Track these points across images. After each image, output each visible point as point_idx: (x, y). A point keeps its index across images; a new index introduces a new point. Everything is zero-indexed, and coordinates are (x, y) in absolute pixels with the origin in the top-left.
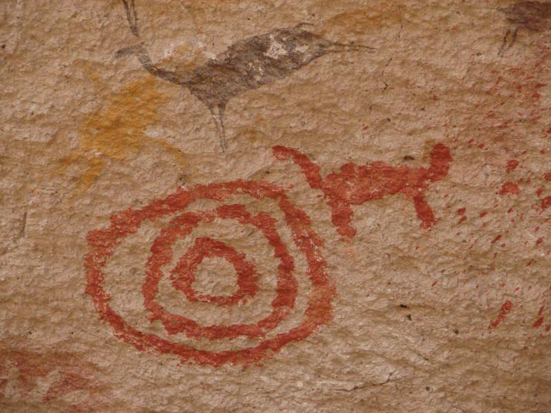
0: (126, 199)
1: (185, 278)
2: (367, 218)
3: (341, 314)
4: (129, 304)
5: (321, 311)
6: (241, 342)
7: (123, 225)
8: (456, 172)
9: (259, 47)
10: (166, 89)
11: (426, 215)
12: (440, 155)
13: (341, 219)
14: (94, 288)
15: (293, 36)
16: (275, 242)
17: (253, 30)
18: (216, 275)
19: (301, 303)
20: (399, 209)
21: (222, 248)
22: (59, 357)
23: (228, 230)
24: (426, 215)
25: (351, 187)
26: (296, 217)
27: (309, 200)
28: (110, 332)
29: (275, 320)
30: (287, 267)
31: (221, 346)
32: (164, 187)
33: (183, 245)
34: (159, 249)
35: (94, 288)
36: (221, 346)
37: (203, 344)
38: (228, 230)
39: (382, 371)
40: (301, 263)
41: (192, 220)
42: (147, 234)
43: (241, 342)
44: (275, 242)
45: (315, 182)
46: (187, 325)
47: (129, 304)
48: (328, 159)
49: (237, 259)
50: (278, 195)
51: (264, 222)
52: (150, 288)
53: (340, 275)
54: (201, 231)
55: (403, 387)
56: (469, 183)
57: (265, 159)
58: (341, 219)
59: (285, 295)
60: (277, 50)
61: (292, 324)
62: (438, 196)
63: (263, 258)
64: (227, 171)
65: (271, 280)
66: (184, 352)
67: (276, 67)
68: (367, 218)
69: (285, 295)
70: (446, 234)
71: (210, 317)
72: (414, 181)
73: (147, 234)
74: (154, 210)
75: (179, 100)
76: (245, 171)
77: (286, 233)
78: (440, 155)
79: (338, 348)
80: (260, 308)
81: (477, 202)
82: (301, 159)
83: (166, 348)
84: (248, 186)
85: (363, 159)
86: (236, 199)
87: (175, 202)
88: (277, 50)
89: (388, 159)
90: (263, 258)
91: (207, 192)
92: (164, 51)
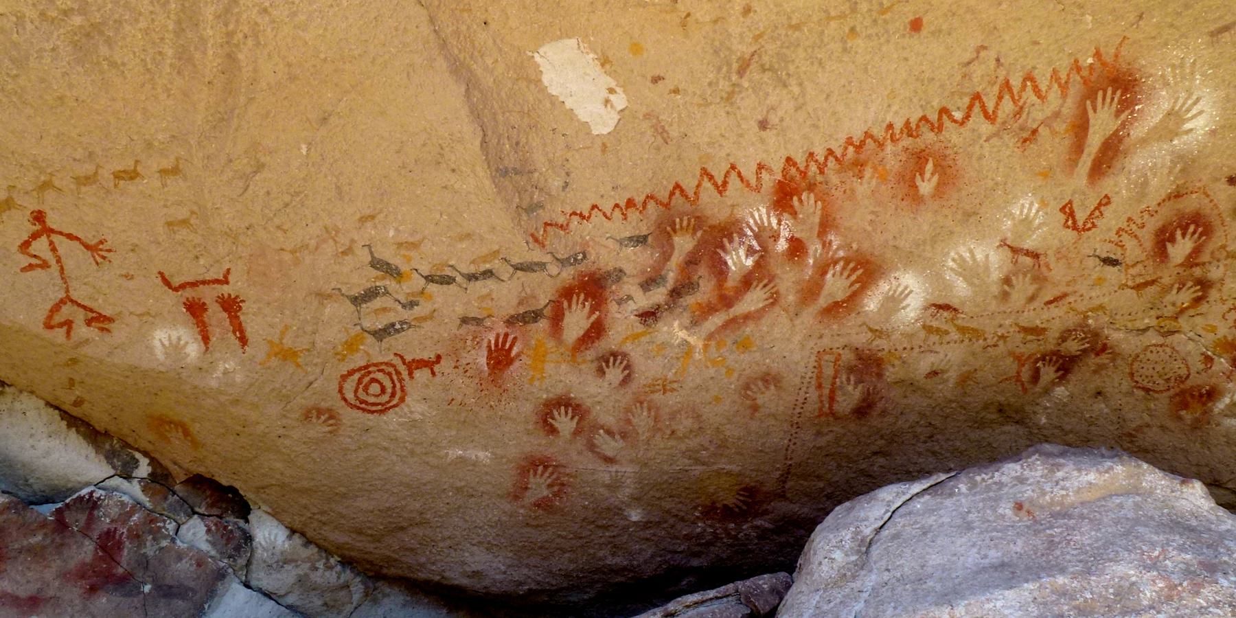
0: (352, 366)
1: (366, 389)
2: (417, 374)
3: (408, 399)
4: (350, 396)
5: (402, 400)
6: (379, 407)
7: (351, 373)
8: (443, 362)
9: (393, 325)
10: (366, 335)
11: (433, 373)
12: (439, 358)
13: (411, 374)
14: (340, 391)
15: (402, 323)
16: (392, 380)
17: (393, 320)
18: (375, 388)
19: (397, 397)
20: (427, 371)
21: (377, 381)
22: (329, 410)
23: (379, 376)
24: (433, 373)
25: (415, 365)
26: (398, 373)
27: (402, 369)
28: (343, 403)
29: (388, 402)
30: (394, 386)
31: (374, 408)
32: (363, 363)
33: (367, 379)
34: (360, 381)
35: (340, 391)
36: (374, 408)
37: (369, 408)
38: (379, 376)
39: (418, 417)
40: (398, 385)
41: (370, 373)
42: (357, 376)
43: (379, 407)
44: (392, 380)
45: (404, 363)
46: (366, 403)
47: (350, 396)
48: (408, 358)
49: (381, 384)
50: (394, 366)
51: (389, 374)
52: (356, 391)
53: (408, 388)
54: (372, 376)
55: (423, 421)
56: (445, 366)
57: (392, 357)
58: (411, 374)
59: (393, 395)
60: (398, 326)
61: (394, 402)
62: (436, 368)
63: (388, 384)
64: (381, 359)
65: (389, 390)
66: (364, 410)
67: (397, 331)
68: (417, 374)
69: (393, 395)
70: (438, 379)
71: (372, 400)
72: (429, 364)
73: (357, 376)
74: (360, 369)
75: (370, 339)
76: (386, 360)
77: (395, 377)
78: (439, 358)
79: (406, 410)
80: (385, 398)
81: (447, 371)
82: (401, 357)
83: (359, 408)
84: (386, 364)
85: (418, 358)
86: (383, 367)
87: (366, 367)
88: (398, 326)
89: (426, 358)
90: (388, 384)
91: (375, 365)
92: (367, 324)
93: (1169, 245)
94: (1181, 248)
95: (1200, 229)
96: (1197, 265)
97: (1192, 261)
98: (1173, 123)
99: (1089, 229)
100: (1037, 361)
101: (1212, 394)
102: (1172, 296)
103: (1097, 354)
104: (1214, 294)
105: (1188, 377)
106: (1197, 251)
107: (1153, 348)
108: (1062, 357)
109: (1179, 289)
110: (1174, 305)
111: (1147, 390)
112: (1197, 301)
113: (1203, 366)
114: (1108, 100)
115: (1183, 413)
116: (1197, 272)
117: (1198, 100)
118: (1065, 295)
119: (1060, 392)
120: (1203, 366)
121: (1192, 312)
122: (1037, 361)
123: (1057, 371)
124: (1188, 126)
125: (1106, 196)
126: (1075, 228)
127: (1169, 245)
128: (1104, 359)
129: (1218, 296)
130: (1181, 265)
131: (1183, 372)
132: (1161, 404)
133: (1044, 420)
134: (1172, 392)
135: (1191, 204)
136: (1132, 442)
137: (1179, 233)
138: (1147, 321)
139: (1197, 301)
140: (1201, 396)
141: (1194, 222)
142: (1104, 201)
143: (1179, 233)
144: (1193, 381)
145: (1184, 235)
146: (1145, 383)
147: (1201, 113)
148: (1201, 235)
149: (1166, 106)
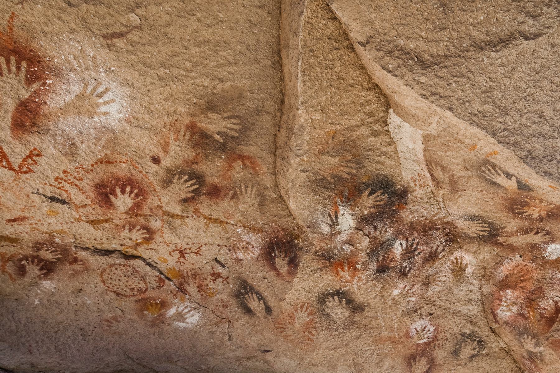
93: (112, 198)
94: (123, 201)
95: (136, 191)
96: (141, 215)
97: (134, 211)
98: (84, 105)
99: (26, 172)
100: (21, 260)
101: (164, 305)
102: (125, 233)
103: (71, 263)
104: (157, 238)
105: (146, 290)
106: (137, 206)
107: (118, 267)
108: (43, 260)
109: (130, 230)
110: (131, 239)
111: (118, 294)
112: (147, 240)
113: (157, 284)
114: (14, 69)
115: (146, 312)
116: (142, 220)
117: (107, 90)
118: (23, 219)
119: (47, 284)
120: (157, 284)
121: (146, 246)
122: (21, 260)
123: (41, 269)
124: (103, 109)
125: (35, 149)
126: (11, 168)
127: (112, 198)
128: (77, 267)
129: (161, 240)
130: (127, 213)
131: (142, 285)
132: (129, 305)
133: (37, 302)
134: (136, 298)
135: (122, 170)
136: (108, 326)
137: (118, 190)
138: (114, 246)
139: (147, 240)
140: (157, 304)
141: (129, 184)
142: (36, 152)
143: (118, 190)
144: (150, 293)
145: (123, 192)
146: (115, 289)
147: (113, 101)
148: (137, 196)
149: (76, 89)
